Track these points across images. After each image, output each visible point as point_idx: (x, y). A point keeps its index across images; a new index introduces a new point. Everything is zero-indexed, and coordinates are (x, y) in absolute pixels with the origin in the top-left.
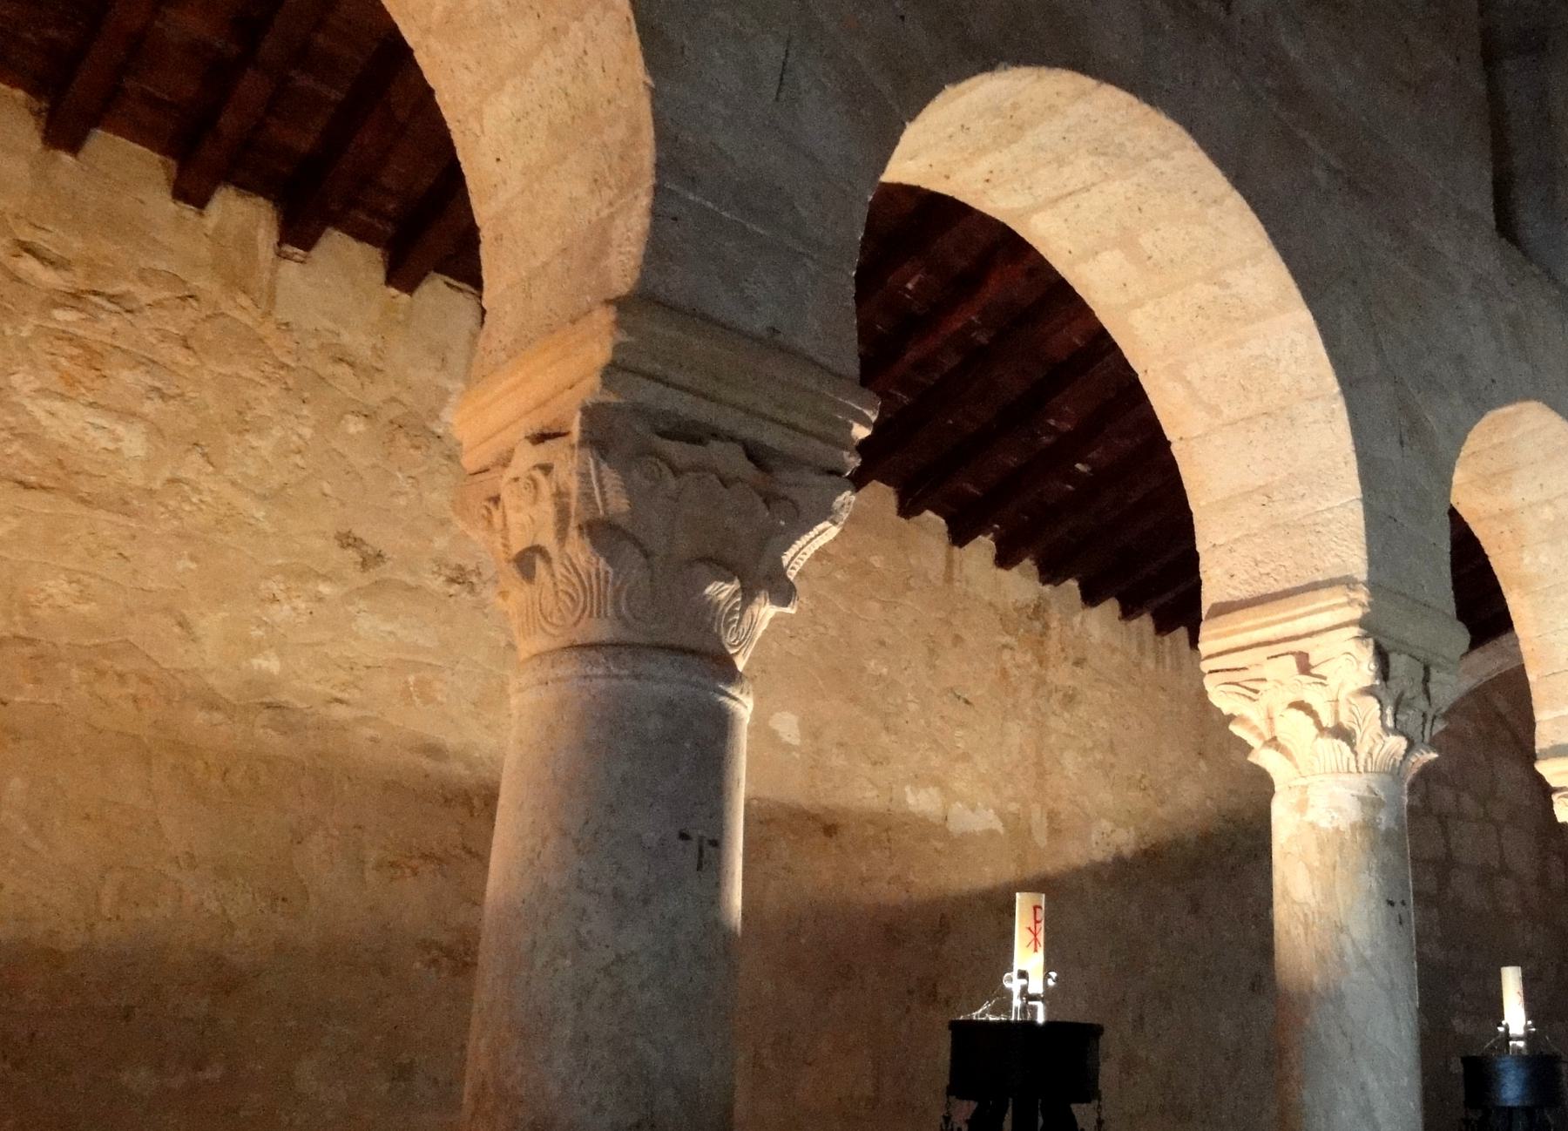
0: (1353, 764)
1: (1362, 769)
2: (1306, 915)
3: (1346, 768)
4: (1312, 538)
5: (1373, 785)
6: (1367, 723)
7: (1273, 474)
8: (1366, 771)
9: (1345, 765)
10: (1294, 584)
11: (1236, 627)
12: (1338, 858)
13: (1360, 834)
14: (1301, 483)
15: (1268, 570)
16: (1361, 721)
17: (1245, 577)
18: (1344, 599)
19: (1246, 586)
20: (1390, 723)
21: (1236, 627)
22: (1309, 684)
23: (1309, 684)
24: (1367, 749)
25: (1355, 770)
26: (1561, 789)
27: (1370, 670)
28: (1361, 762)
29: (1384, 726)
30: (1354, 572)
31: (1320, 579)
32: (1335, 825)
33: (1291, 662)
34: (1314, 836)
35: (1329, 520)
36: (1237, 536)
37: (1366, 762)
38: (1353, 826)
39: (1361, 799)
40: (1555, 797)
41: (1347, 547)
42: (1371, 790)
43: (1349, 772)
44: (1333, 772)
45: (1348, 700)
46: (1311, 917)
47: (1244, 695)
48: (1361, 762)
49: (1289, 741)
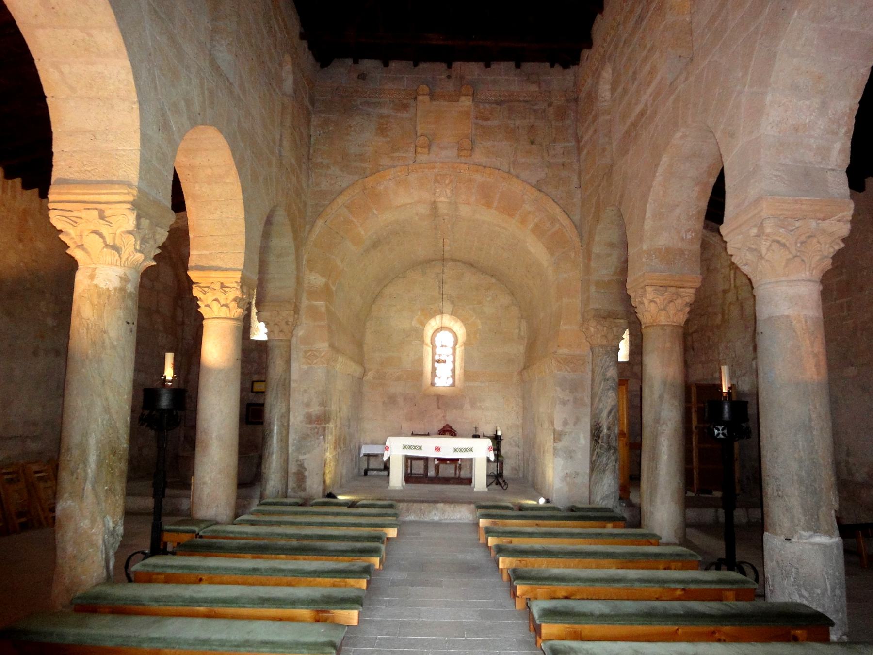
0: (119, 263)
1: (122, 265)
8: (124, 266)
12: (107, 301)
18: (126, 191)
20: (138, 248)
24: (126, 257)
26: (197, 283)
29: (135, 249)
32: (107, 287)
38: (115, 289)
39: (120, 277)
40: (194, 286)
42: (125, 274)
44: (109, 264)
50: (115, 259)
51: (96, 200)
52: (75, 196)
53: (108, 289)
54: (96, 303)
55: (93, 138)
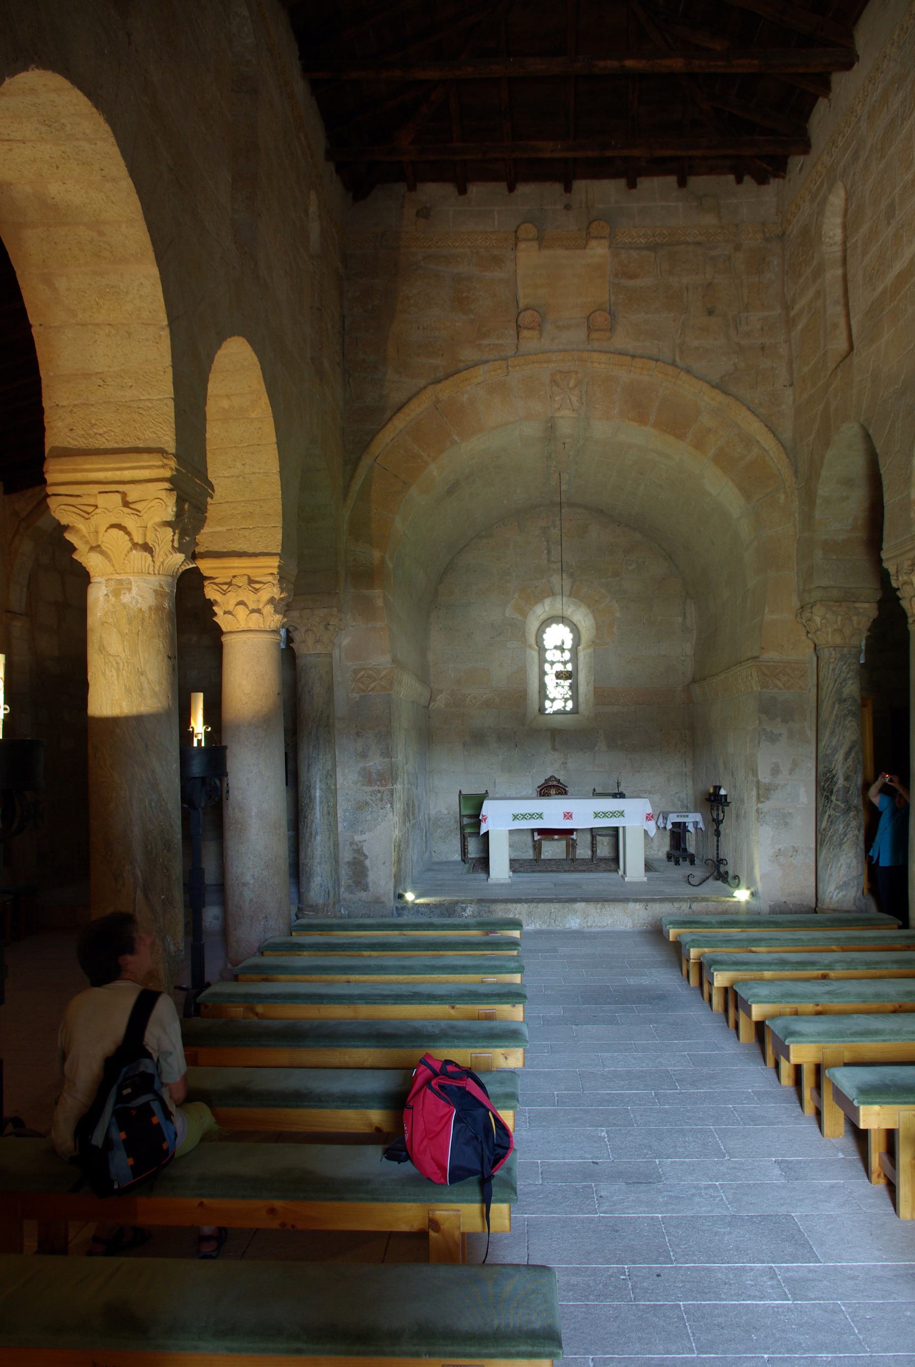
0: (151, 569)
1: (156, 572)
2: (117, 663)
3: (147, 571)
4: (136, 416)
5: (162, 583)
6: (163, 544)
7: (110, 367)
8: (159, 574)
9: (147, 569)
10: (121, 446)
11: (78, 467)
12: (140, 628)
13: (154, 614)
14: (130, 378)
15: (101, 431)
16: (160, 542)
17: (83, 432)
18: (160, 463)
19: (83, 440)
20: (176, 545)
21: (78, 467)
22: (128, 514)
23: (128, 514)
24: (161, 560)
25: (153, 573)
27: (172, 511)
28: (157, 567)
29: (173, 547)
30: (166, 445)
31: (141, 445)
32: (139, 606)
33: (118, 497)
34: (125, 613)
35: (149, 407)
36: (76, 402)
37: (159, 567)
38: (150, 608)
39: (155, 591)
41: (161, 428)
42: (161, 586)
43: (149, 573)
44: (138, 573)
45: (154, 527)
46: (121, 665)
47: (79, 514)
48: (157, 567)
49: (109, 549)
50: (147, 565)
51: (117, 479)
52: (85, 474)
53: (141, 609)
54: (127, 631)
55: (102, 383)
